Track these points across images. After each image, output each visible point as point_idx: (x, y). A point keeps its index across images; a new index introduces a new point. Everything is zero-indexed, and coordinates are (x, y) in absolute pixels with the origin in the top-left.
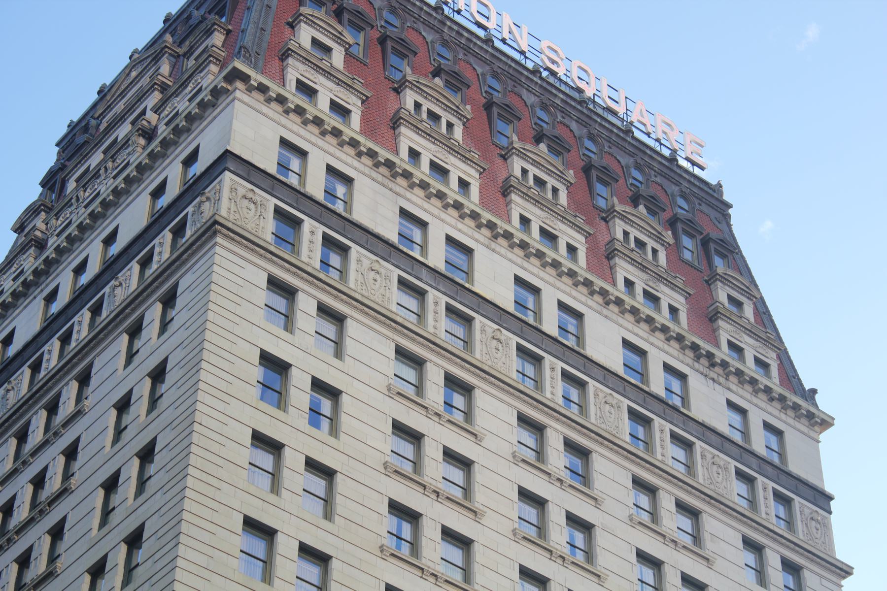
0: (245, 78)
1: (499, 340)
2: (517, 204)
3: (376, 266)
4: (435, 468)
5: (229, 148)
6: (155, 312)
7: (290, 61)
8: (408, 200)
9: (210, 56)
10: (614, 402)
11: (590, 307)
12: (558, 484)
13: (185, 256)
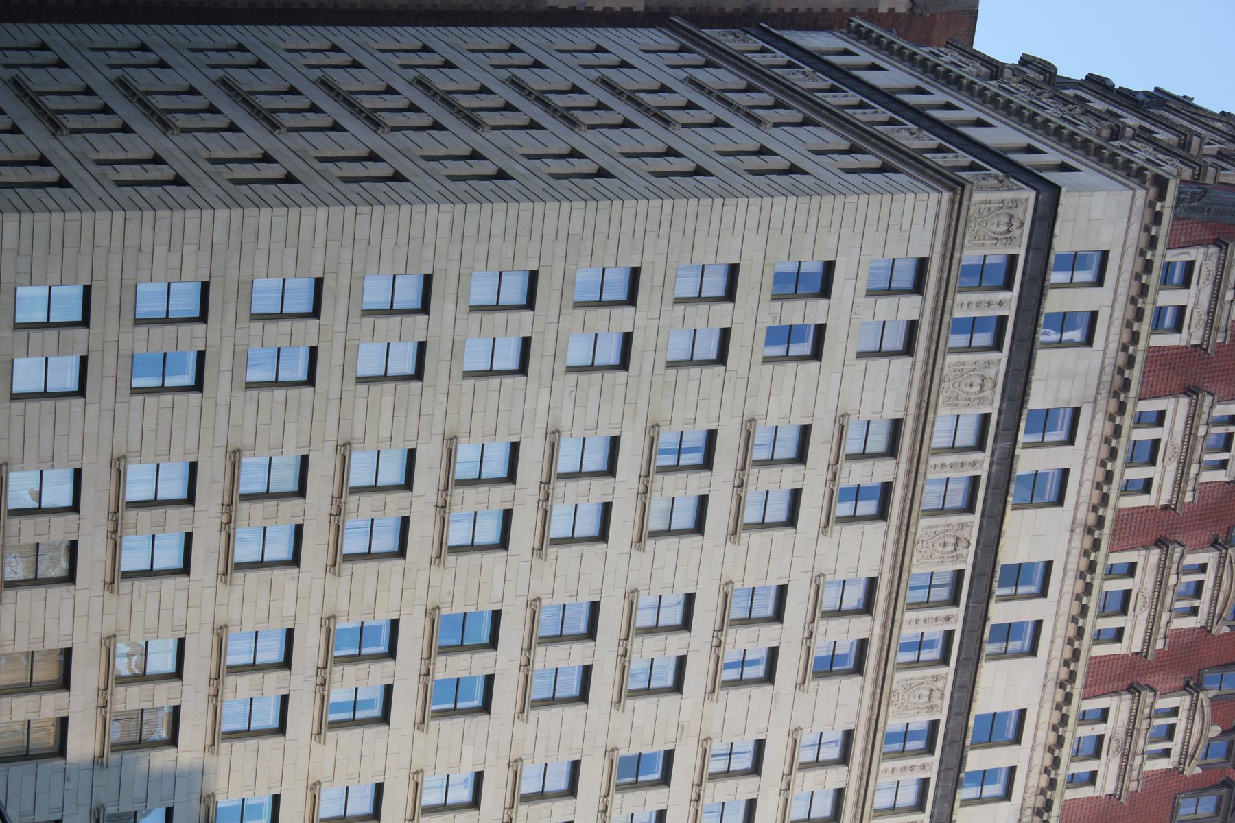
0: (1161, 196)
1: (956, 545)
2: (1147, 558)
3: (989, 384)
4: (775, 484)
5: (1063, 189)
6: (871, 161)
7: (1213, 250)
8: (1093, 417)
9: (1200, 166)
10: (935, 701)
11: (1049, 663)
12: (806, 635)
13: (929, 171)
